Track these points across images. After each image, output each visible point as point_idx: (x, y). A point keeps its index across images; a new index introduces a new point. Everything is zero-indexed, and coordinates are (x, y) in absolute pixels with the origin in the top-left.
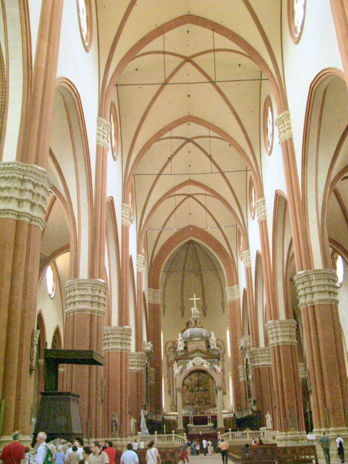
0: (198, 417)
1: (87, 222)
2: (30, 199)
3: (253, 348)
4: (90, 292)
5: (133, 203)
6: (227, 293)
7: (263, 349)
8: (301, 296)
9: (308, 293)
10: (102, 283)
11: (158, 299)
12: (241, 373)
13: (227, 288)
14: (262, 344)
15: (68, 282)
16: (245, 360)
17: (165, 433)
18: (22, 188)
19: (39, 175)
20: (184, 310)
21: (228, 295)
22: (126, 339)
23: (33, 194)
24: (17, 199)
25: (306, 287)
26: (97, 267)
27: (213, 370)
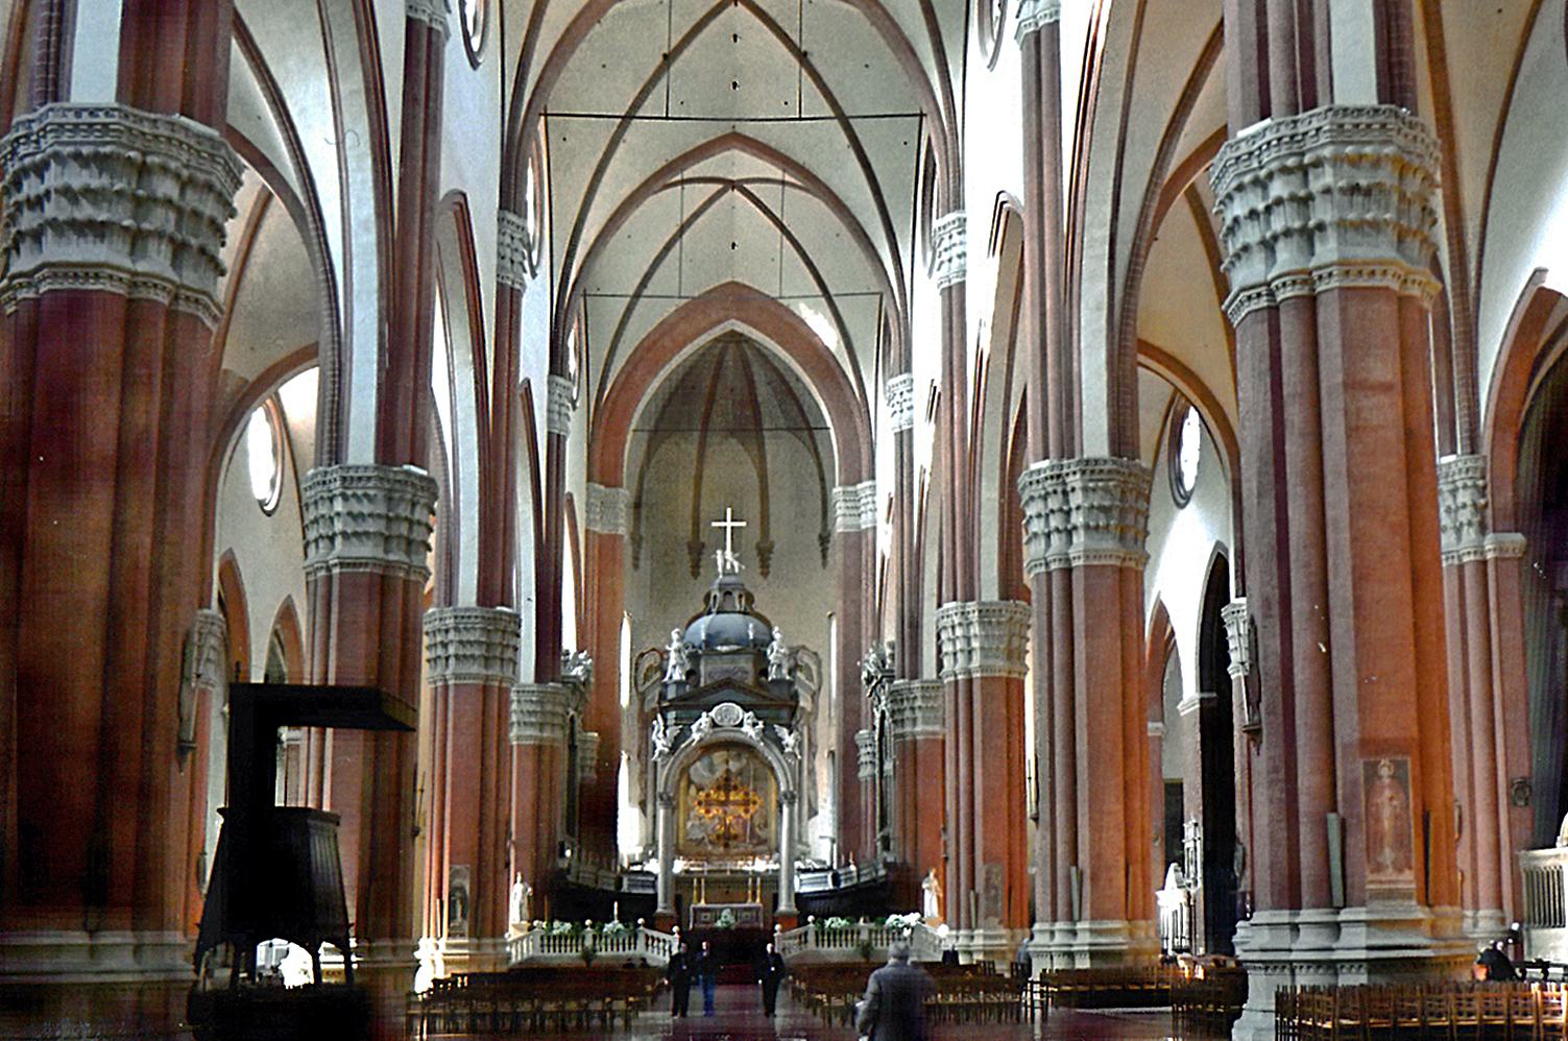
1: (375, 284)
2: (171, 228)
4: (381, 509)
5: (542, 206)
8: (1035, 535)
9: (1058, 530)
10: (421, 478)
14: (929, 671)
15: (311, 472)
16: (878, 715)
18: (141, 192)
19: (198, 152)
20: (700, 553)
21: (839, 512)
23: (180, 211)
24: (126, 229)
25: (1052, 511)
26: (403, 427)
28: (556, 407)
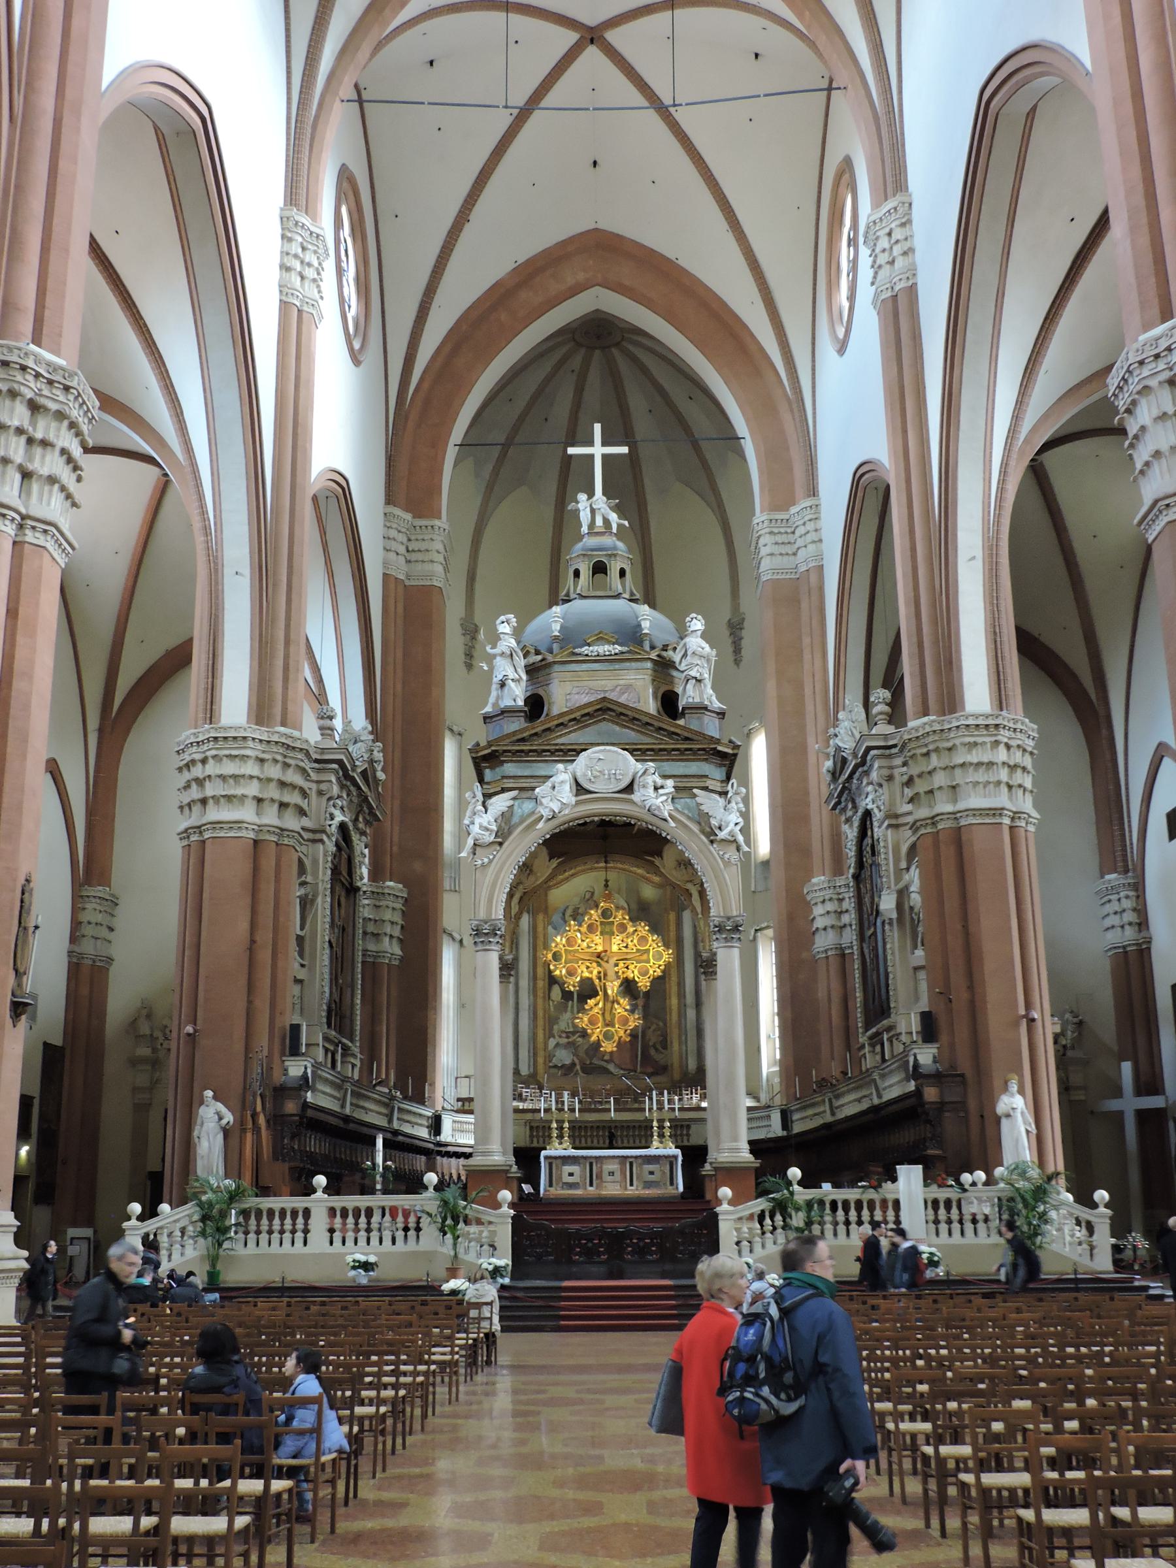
0: (612, 1121)
3: (926, 719)
6: (762, 541)
7: (980, 721)
11: (432, 561)
12: (821, 916)
13: (760, 517)
16: (850, 833)
17: (379, 1187)
21: (764, 551)
22: (30, 441)
27: (695, 828)
28: (297, 265)
